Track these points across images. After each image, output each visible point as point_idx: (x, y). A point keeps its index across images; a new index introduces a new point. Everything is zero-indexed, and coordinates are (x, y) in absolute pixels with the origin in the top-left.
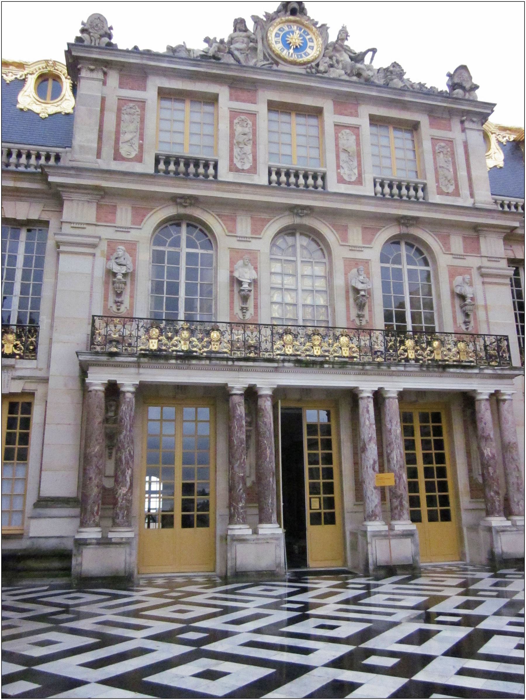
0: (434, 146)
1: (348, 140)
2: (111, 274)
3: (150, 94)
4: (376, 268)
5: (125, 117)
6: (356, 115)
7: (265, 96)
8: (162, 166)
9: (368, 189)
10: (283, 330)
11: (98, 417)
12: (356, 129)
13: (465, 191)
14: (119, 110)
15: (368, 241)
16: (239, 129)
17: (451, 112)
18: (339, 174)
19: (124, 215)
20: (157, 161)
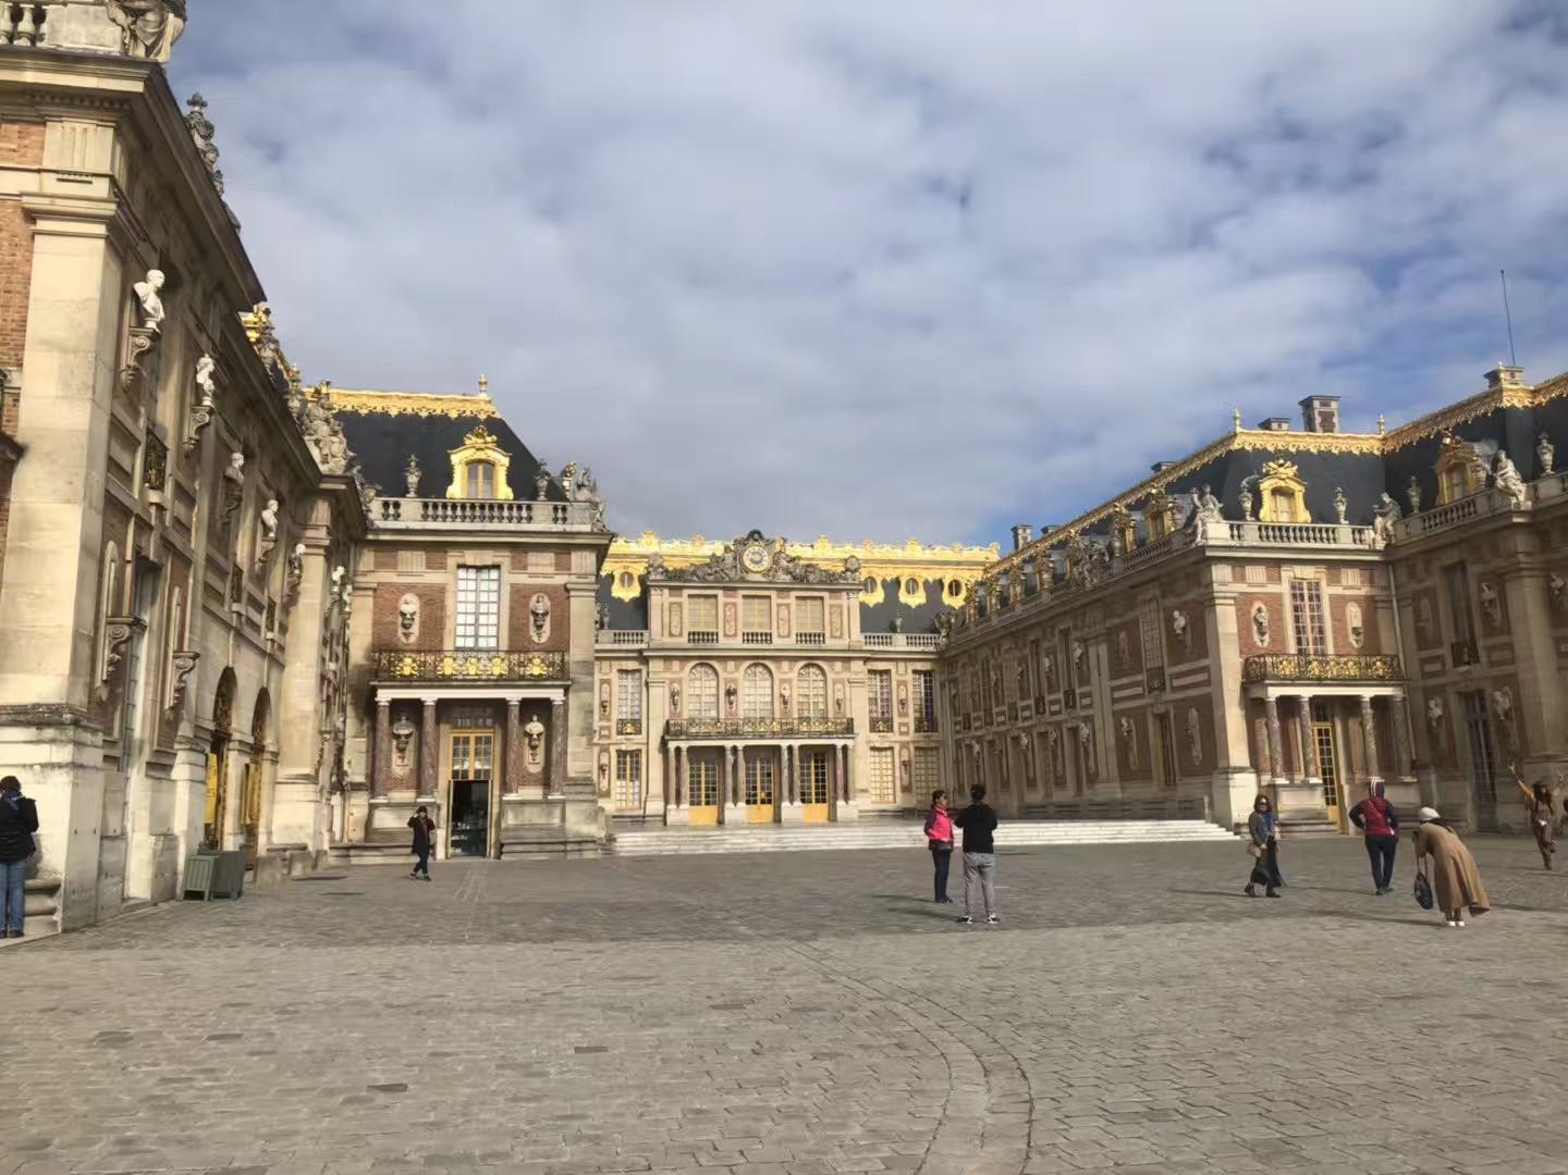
1: (784, 613)
2: (673, 695)
6: (788, 597)
9: (791, 642)
10: (748, 721)
12: (788, 606)
13: (846, 636)
17: (840, 591)
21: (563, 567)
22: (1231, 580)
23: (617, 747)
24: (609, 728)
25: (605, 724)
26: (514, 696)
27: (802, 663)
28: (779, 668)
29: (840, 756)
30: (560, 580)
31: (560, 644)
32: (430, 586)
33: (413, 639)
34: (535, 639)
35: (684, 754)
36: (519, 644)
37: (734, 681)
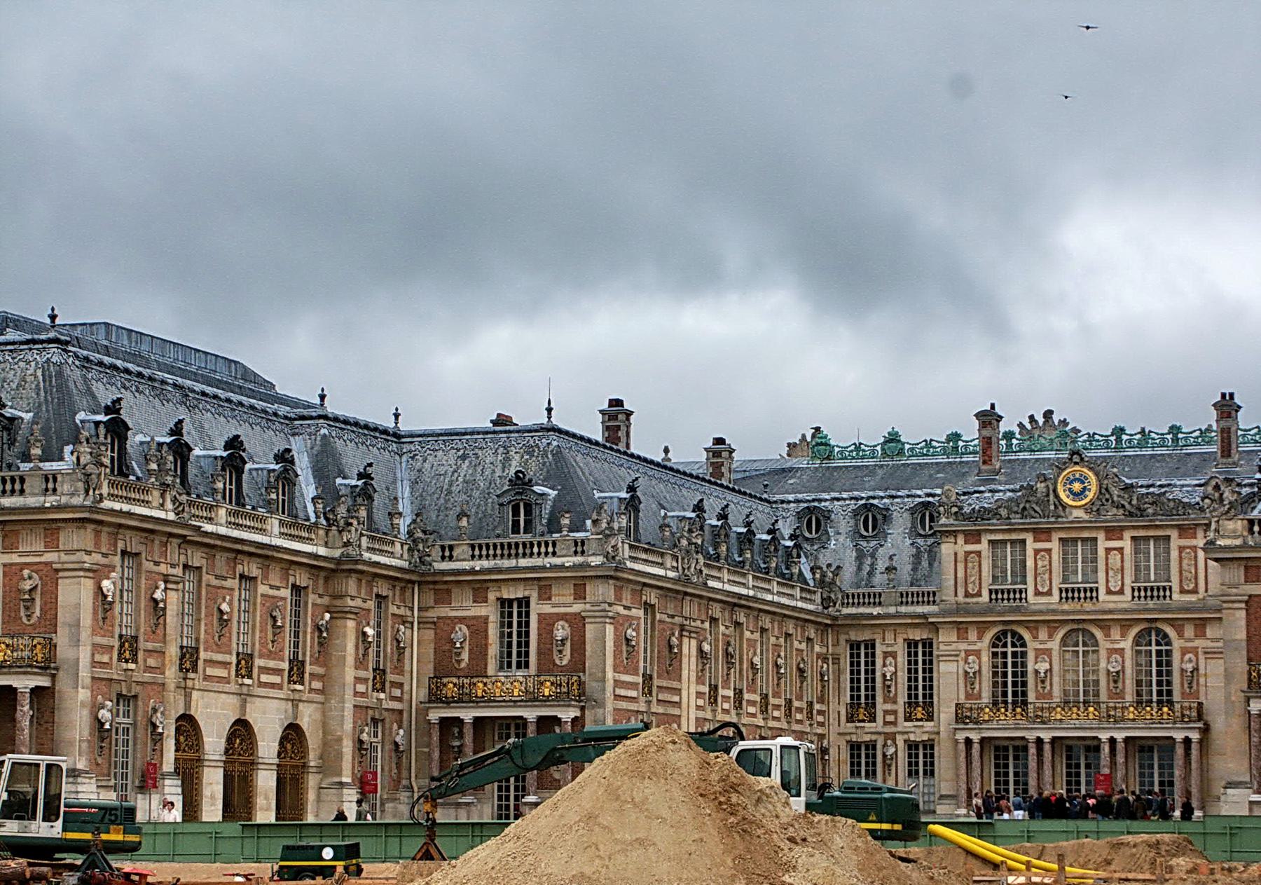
0: (1180, 552)
1: (1115, 557)
2: (966, 673)
3: (983, 546)
4: (1128, 654)
5: (970, 565)
6: (1121, 539)
7: (1056, 536)
8: (994, 596)
9: (1125, 600)
11: (963, 755)
12: (1121, 550)
14: (966, 560)
15: (1123, 635)
16: (1040, 563)
18: (1107, 587)
19: (972, 635)
20: (991, 591)
21: (580, 595)
22: (1242, 580)
23: (906, 737)
24: (895, 712)
25: (889, 707)
26: (531, 714)
27: (1134, 631)
28: (1107, 635)
29: (1180, 751)
30: (577, 608)
31: (578, 664)
32: (474, 618)
33: (463, 665)
34: (558, 662)
35: (976, 748)
36: (547, 666)
37: (1048, 652)
